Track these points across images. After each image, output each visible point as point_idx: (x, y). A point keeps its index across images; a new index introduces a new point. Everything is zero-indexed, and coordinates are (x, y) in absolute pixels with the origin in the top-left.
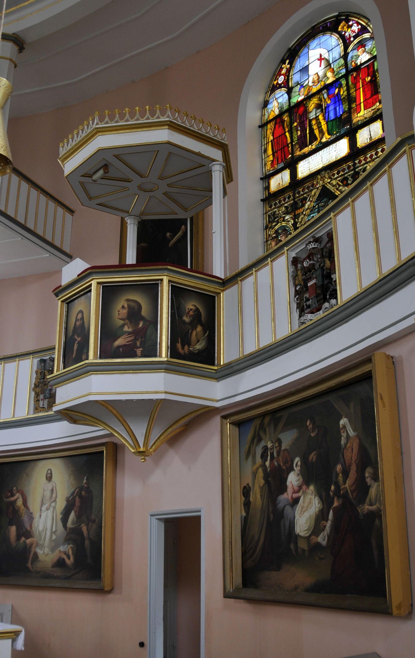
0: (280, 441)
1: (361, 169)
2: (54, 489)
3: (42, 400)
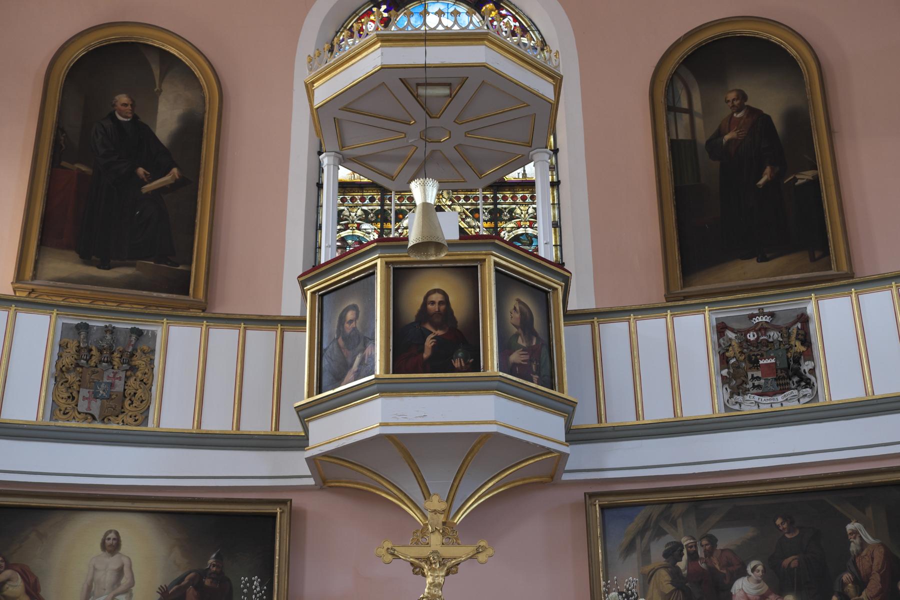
0: (713, 541)
1: (505, 209)
2: (126, 569)
3: (84, 398)
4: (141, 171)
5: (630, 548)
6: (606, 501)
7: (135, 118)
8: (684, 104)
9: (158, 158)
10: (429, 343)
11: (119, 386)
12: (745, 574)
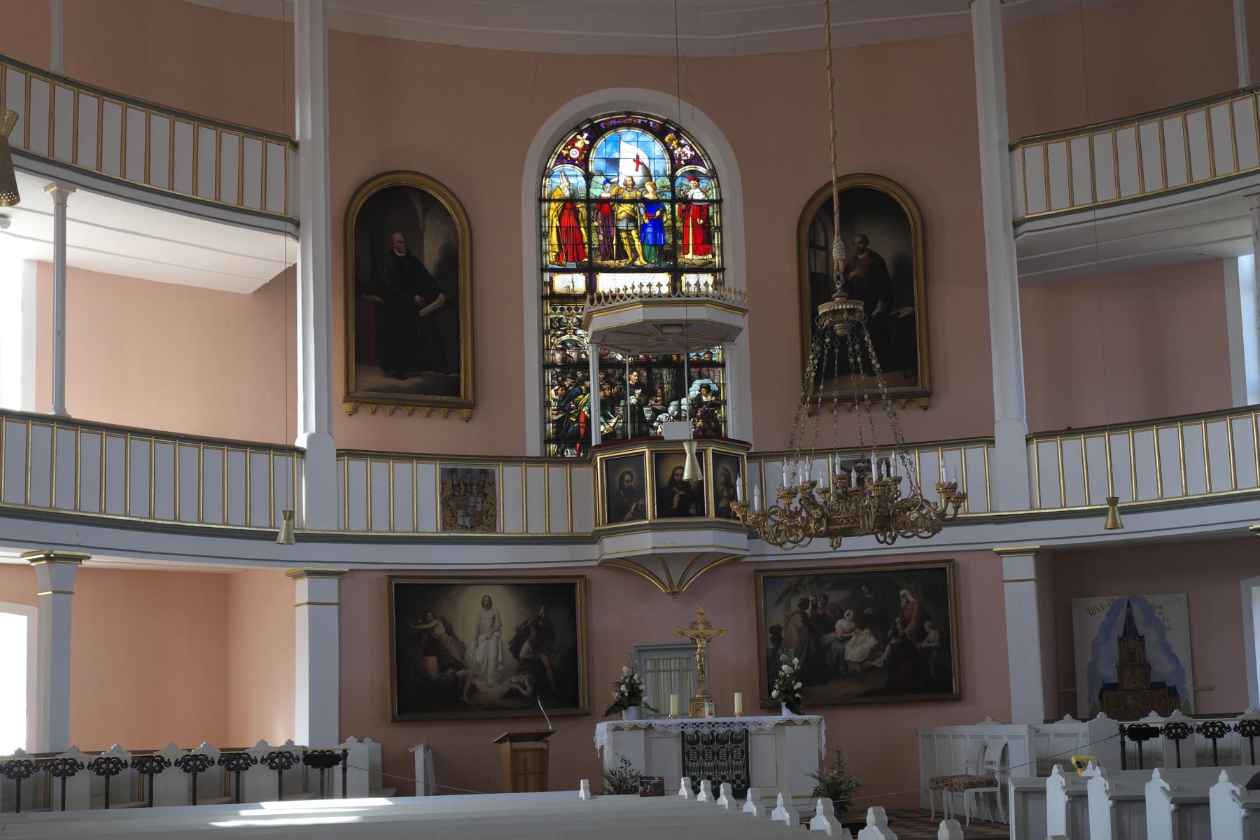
0: (826, 598)
4: (417, 298)
5: (779, 601)
6: (766, 574)
7: (408, 252)
8: (823, 244)
10: (676, 499)
11: (479, 507)
12: (842, 617)
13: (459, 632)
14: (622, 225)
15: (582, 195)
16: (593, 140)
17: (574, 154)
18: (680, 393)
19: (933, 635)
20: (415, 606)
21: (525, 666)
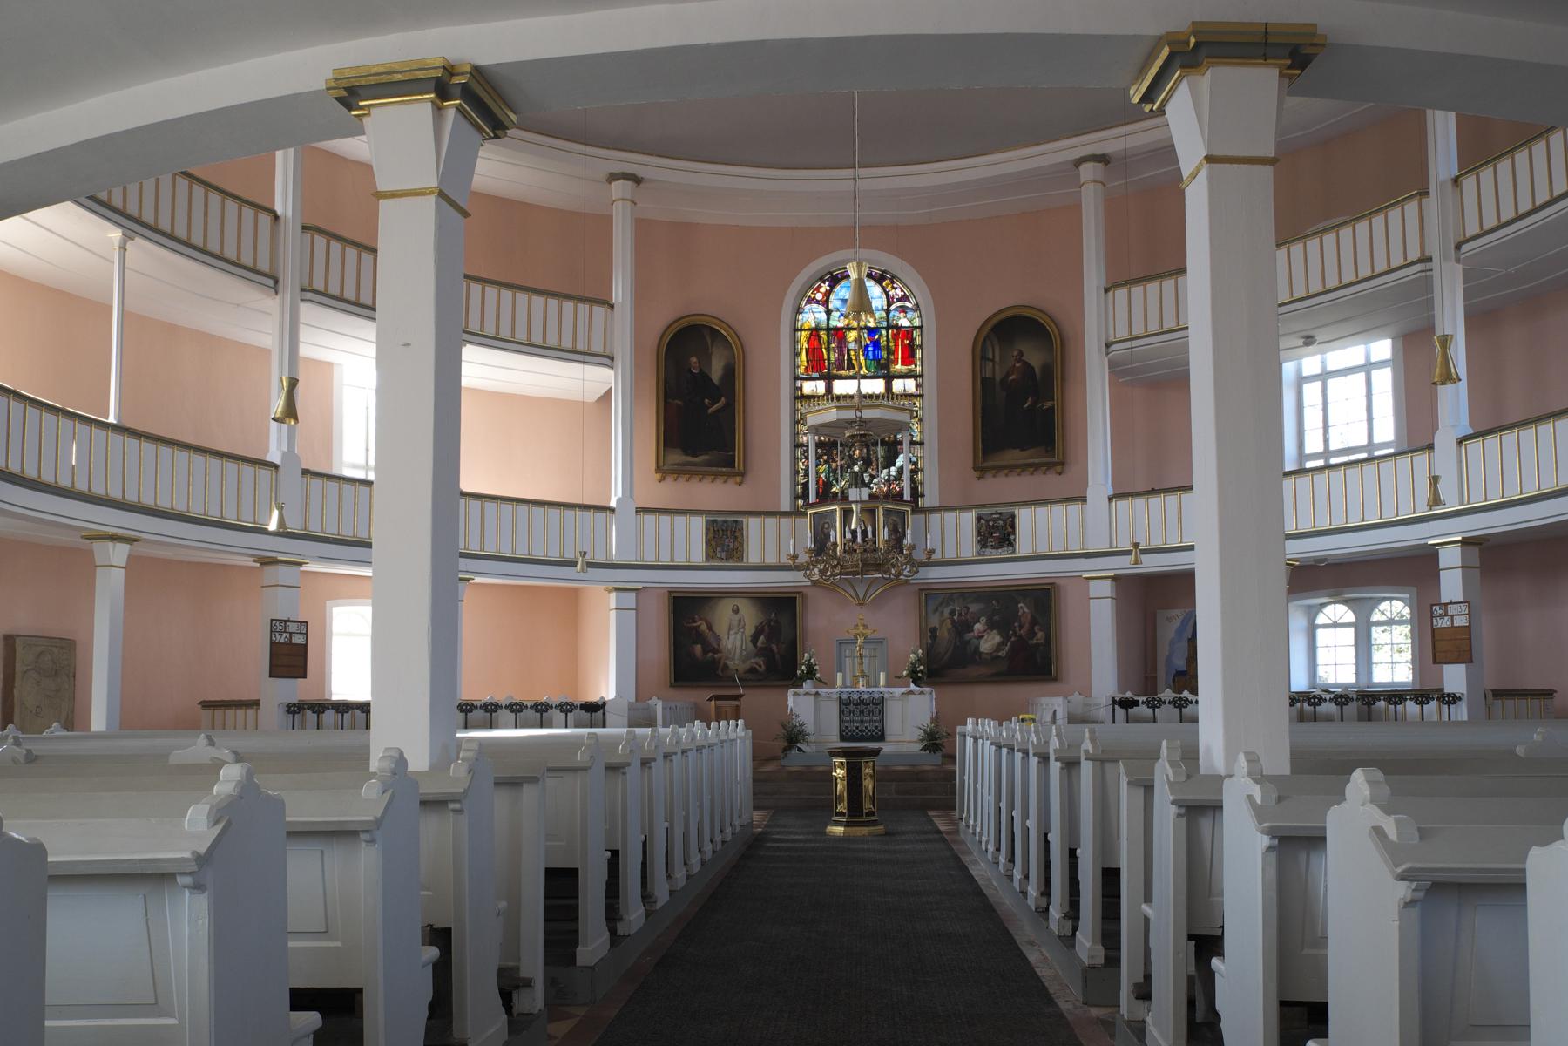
9: (714, 392)
13: (716, 628)
14: (851, 346)
15: (824, 325)
16: (832, 286)
17: (819, 296)
18: (890, 462)
19: (1040, 635)
20: (687, 610)
21: (761, 652)
